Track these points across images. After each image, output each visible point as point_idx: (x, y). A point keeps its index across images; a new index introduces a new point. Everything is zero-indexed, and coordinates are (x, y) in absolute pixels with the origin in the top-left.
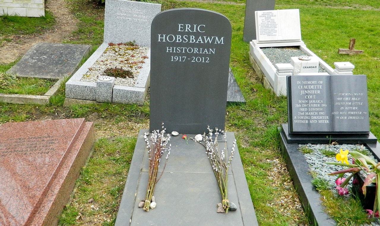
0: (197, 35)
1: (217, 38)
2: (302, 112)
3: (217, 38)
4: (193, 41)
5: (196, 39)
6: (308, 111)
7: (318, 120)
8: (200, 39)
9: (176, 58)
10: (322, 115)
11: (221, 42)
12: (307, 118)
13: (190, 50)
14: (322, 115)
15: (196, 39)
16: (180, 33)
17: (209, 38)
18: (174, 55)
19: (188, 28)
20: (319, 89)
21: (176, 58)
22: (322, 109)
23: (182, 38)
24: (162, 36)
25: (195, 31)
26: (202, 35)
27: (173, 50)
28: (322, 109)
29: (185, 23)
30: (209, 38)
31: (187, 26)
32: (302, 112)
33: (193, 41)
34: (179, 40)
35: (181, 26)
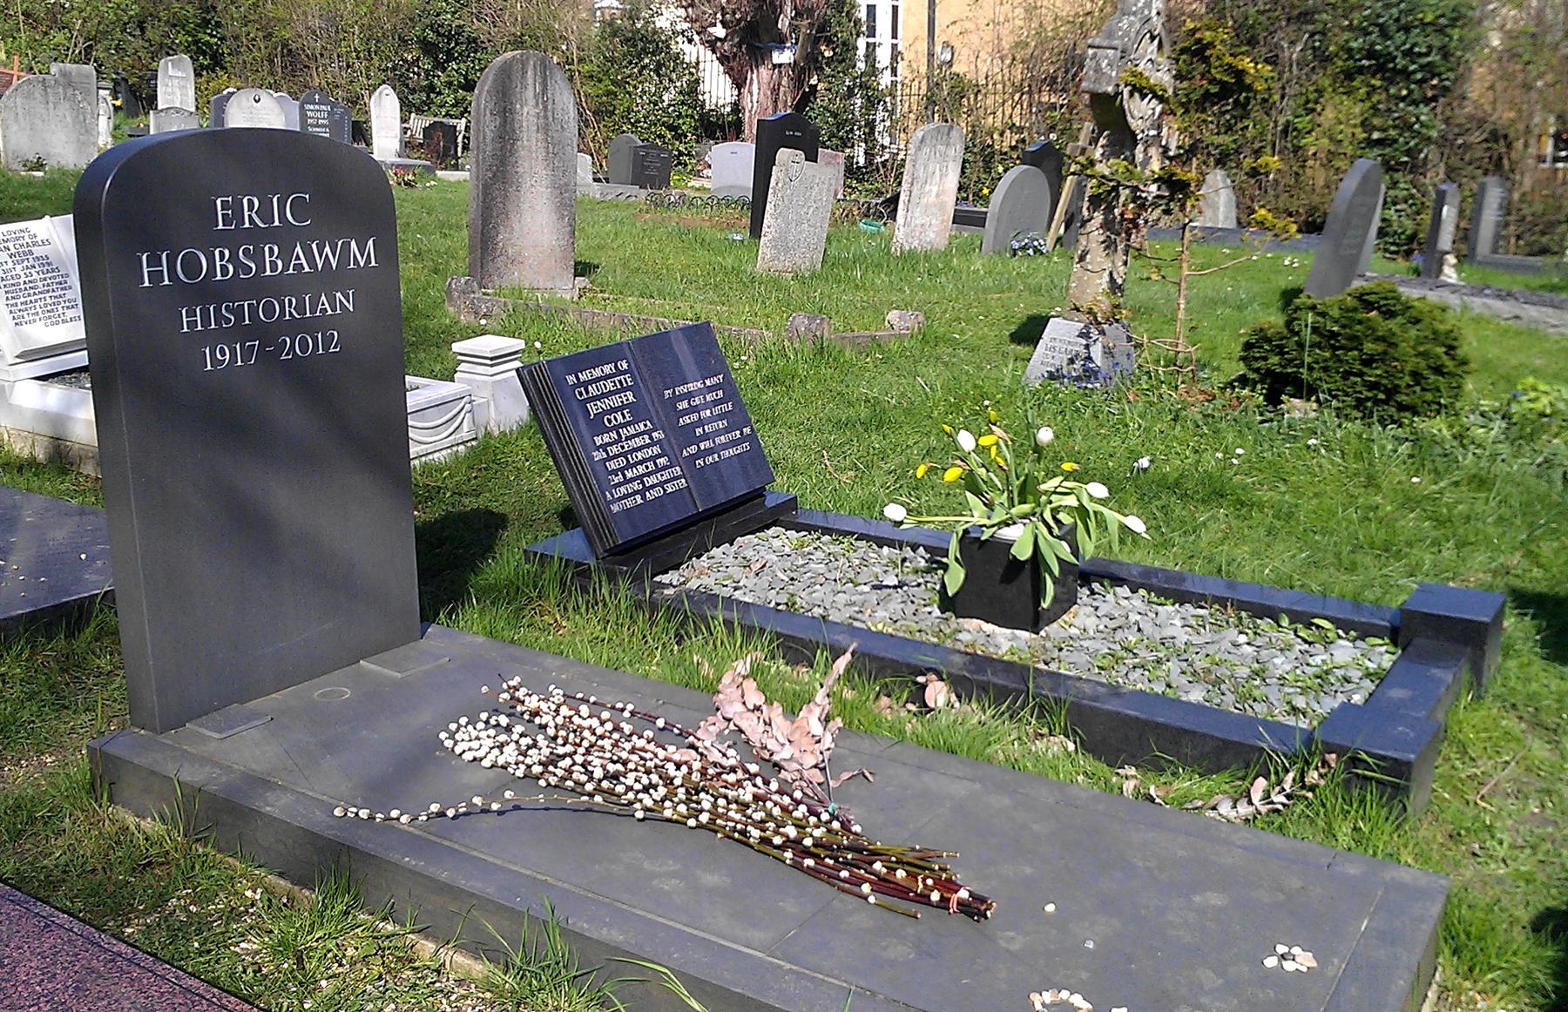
0: (285, 238)
1: (353, 243)
2: (615, 472)
3: (353, 243)
4: (274, 266)
5: (286, 255)
6: (630, 466)
7: (661, 484)
8: (298, 258)
9: (223, 353)
10: (665, 468)
11: (368, 260)
12: (636, 486)
13: (269, 309)
14: (665, 468)
15: (286, 255)
16: (224, 239)
17: (327, 249)
18: (212, 338)
19: (250, 207)
20: (629, 388)
21: (223, 353)
22: (656, 450)
23: (234, 258)
24: (154, 261)
25: (277, 223)
26: (304, 238)
27: (206, 321)
28: (656, 450)
29: (237, 194)
30: (327, 249)
31: (245, 201)
32: (615, 472)
33: (274, 266)
34: (224, 270)
35: (225, 205)
